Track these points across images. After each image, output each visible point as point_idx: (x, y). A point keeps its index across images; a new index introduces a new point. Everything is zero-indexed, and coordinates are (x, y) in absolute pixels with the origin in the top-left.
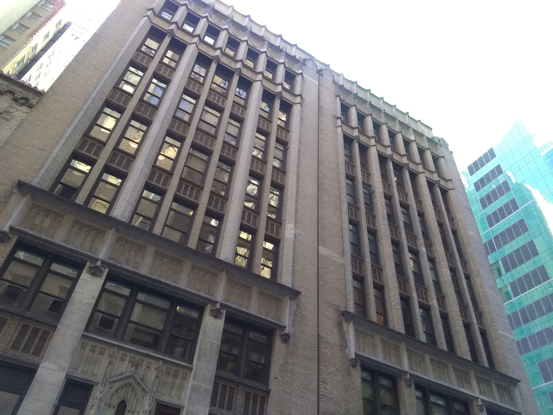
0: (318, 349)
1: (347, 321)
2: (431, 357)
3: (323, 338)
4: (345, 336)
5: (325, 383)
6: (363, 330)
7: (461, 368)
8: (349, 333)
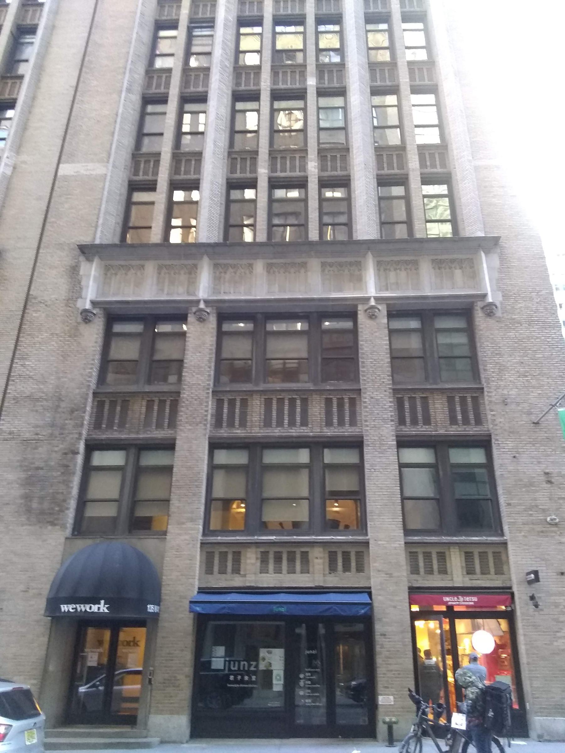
0: (23, 316)
1: (89, 260)
2: (270, 261)
3: (35, 298)
4: (80, 283)
5: (25, 359)
6: (122, 263)
7: (343, 260)
8: (89, 276)
